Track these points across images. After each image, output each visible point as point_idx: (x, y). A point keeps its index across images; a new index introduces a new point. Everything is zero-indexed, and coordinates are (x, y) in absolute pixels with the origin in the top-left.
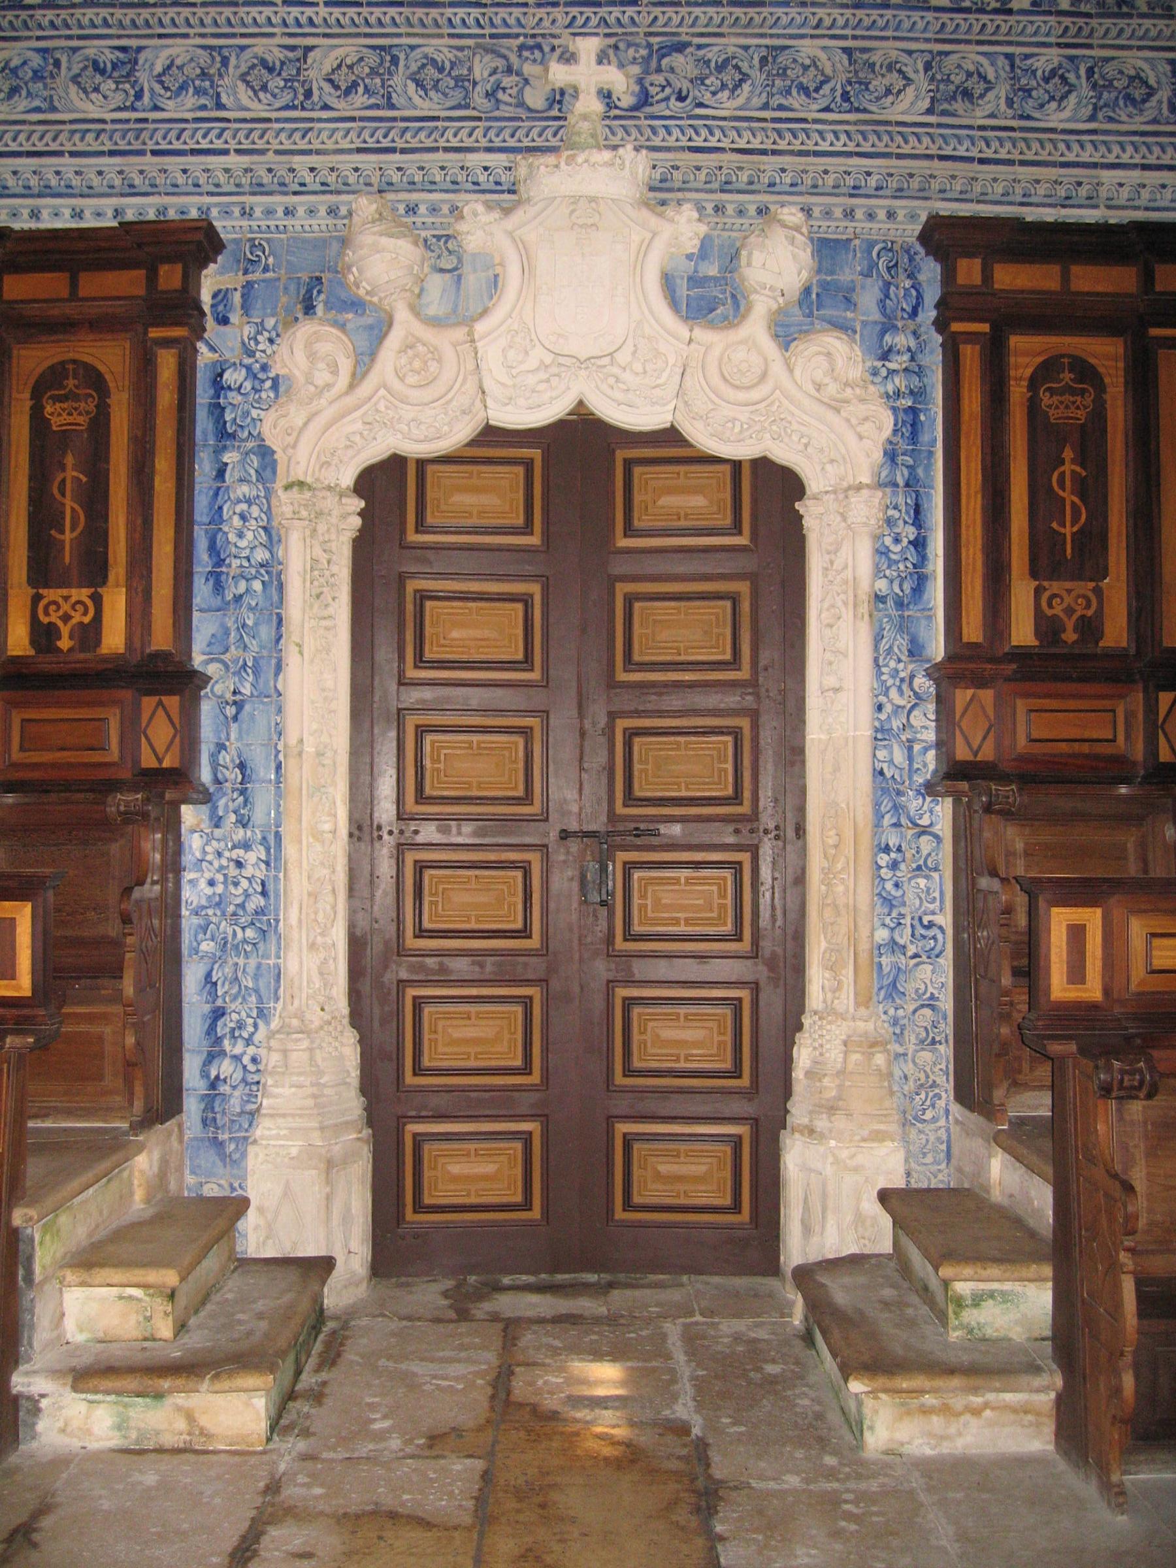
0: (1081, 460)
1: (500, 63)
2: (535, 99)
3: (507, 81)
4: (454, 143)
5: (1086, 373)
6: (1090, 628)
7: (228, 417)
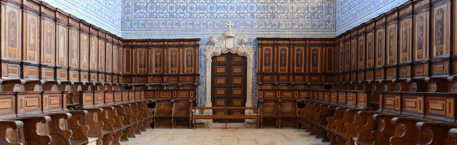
0: (268, 57)
3: (224, 25)
4: (219, 30)
5: (269, 49)
6: (269, 70)
7: (202, 53)
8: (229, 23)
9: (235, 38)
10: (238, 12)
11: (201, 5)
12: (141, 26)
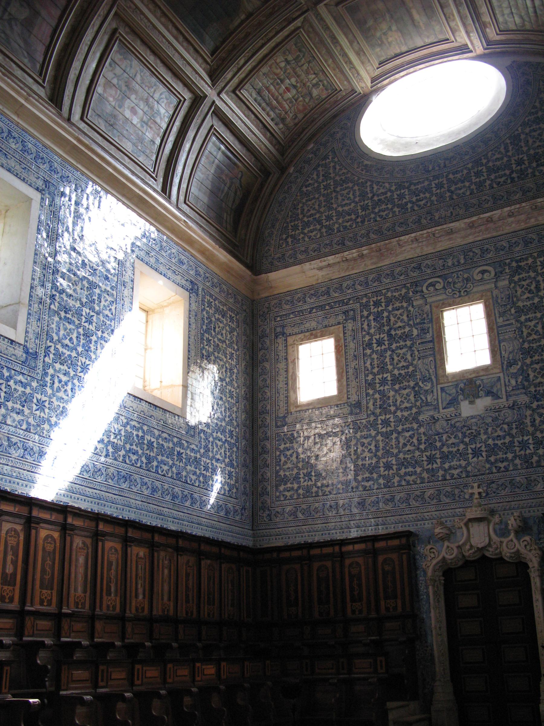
1: (460, 490)
2: (467, 497)
3: (462, 494)
8: (472, 487)
9: (489, 522)
10: (492, 459)
11: (406, 456)
12: (289, 518)
